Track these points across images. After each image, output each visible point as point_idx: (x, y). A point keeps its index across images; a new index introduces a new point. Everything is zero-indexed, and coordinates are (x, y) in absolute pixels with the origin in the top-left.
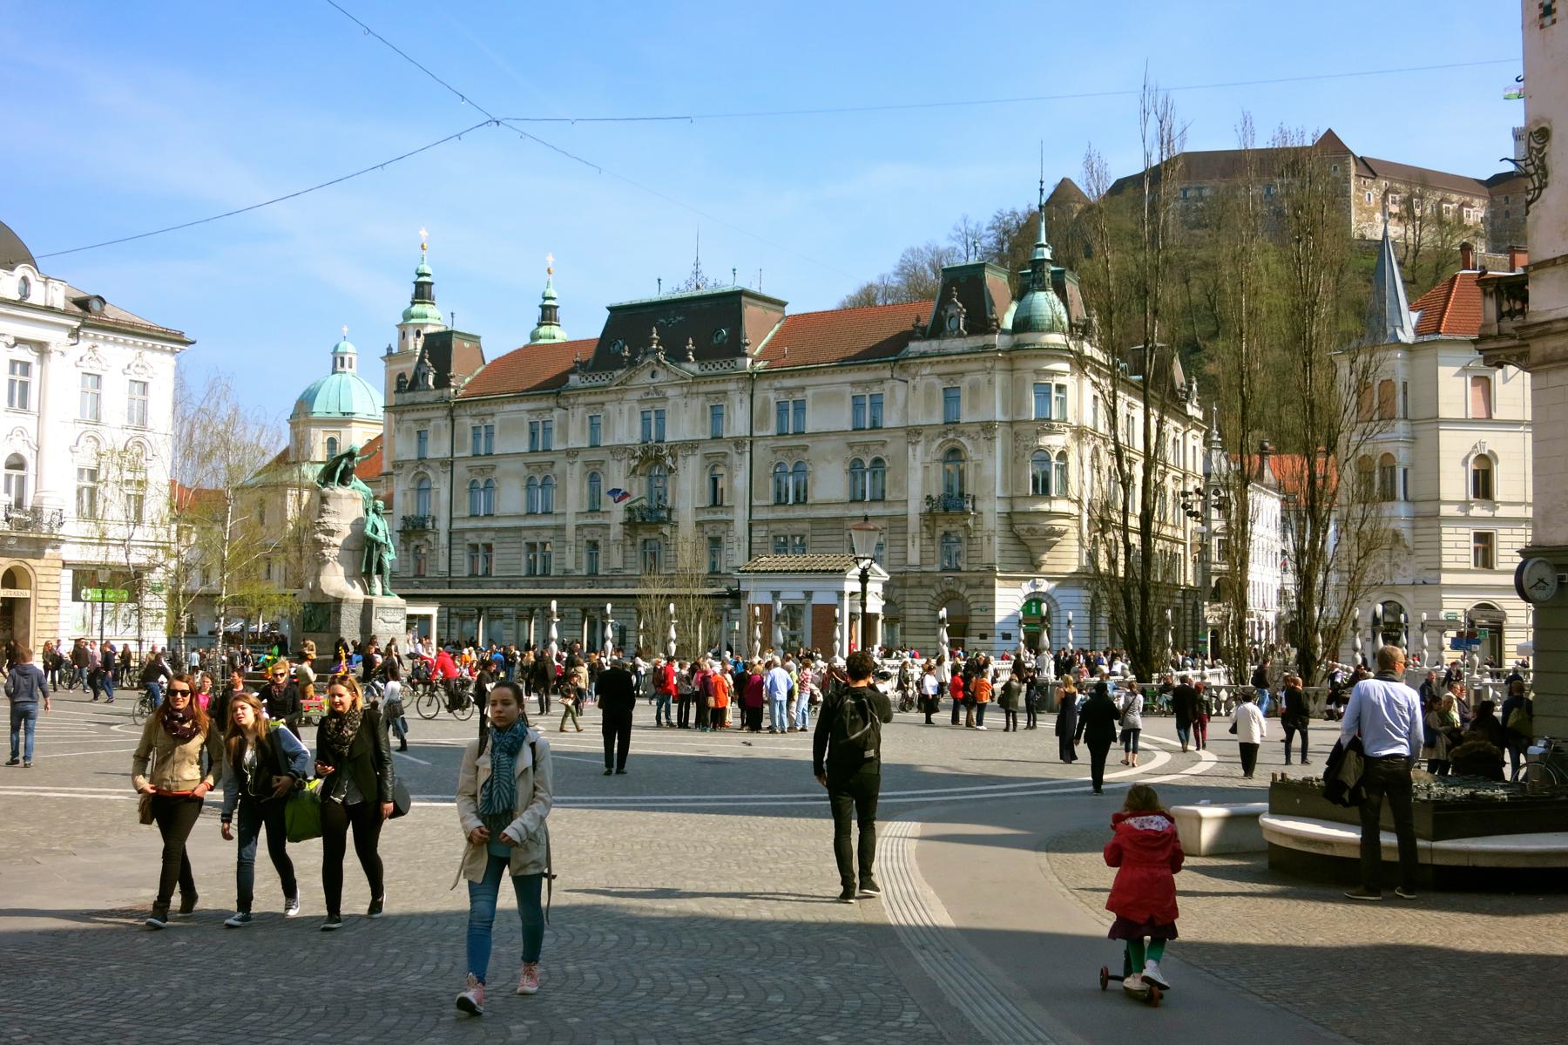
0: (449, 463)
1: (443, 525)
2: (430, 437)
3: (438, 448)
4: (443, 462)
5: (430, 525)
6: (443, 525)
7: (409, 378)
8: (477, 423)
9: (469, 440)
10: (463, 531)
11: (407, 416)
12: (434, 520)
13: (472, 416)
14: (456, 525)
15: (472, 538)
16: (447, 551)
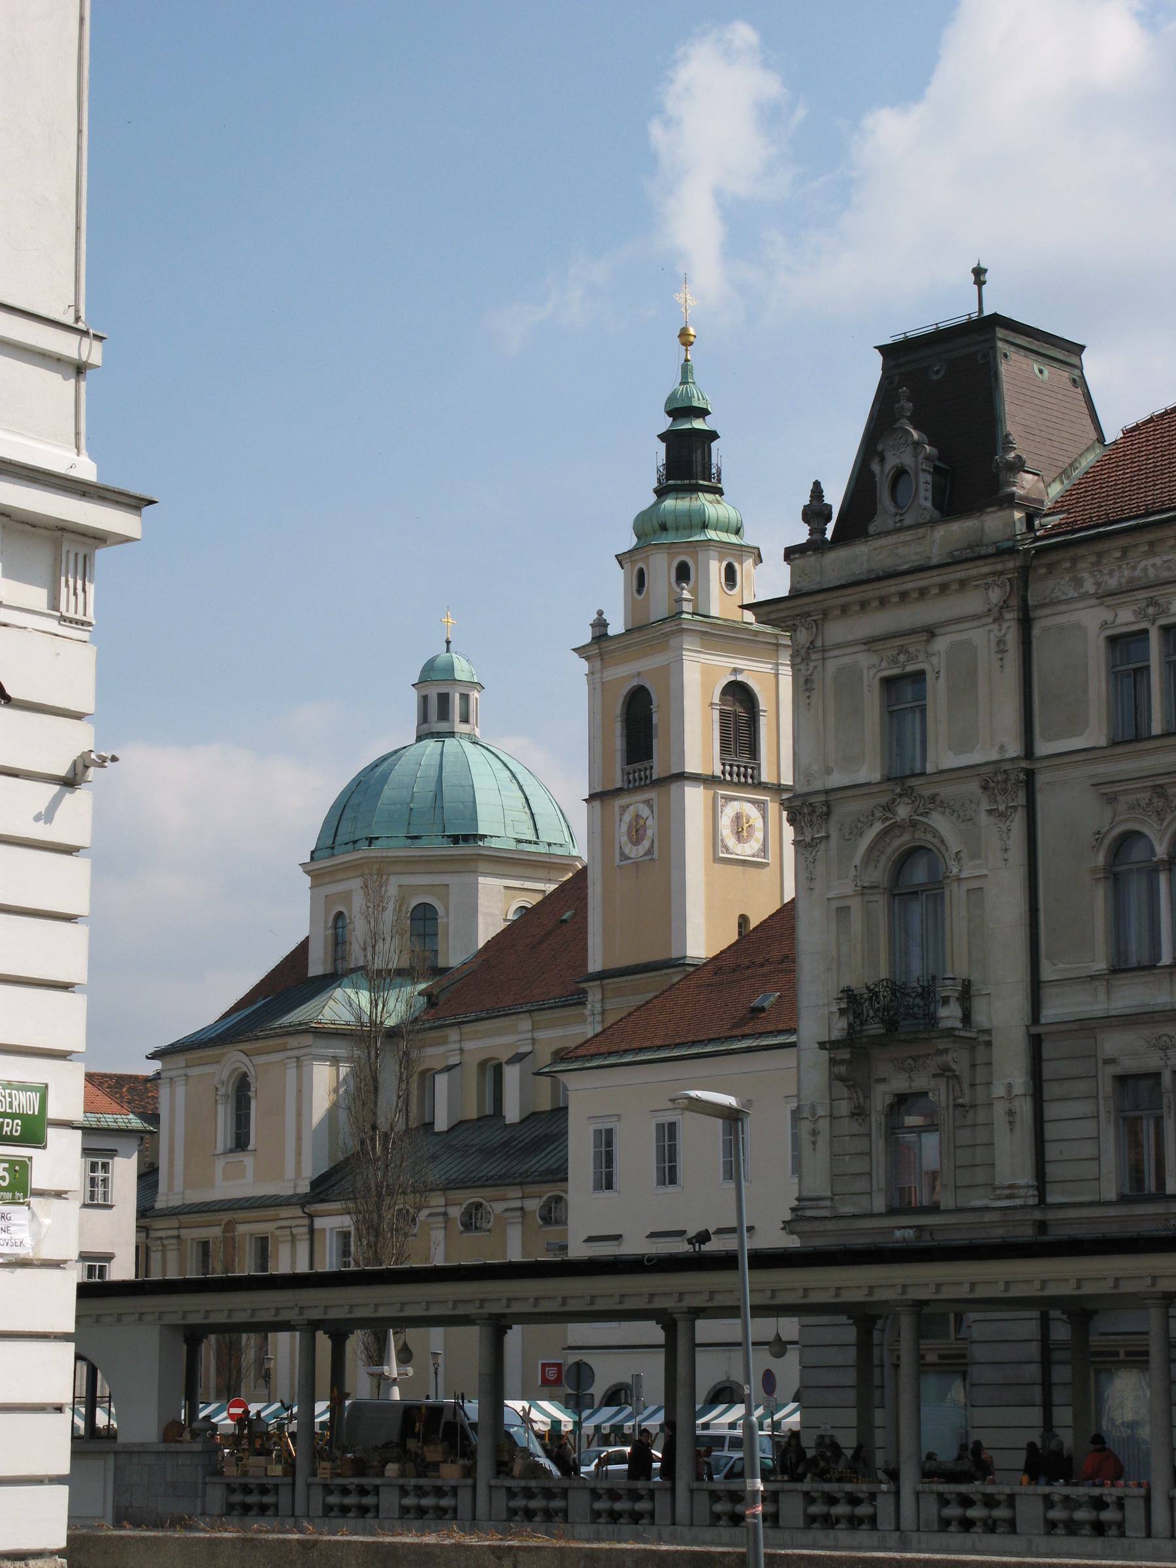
0: (1019, 783)
1: (1003, 1012)
2: (938, 694)
3: (973, 730)
4: (992, 778)
5: (950, 1014)
6: (1003, 1012)
7: (835, 497)
8: (1126, 618)
9: (1098, 685)
10: (1088, 1027)
11: (837, 631)
12: (966, 994)
13: (1104, 596)
14: (1055, 1009)
15: (1128, 1050)
16: (1025, 1108)
